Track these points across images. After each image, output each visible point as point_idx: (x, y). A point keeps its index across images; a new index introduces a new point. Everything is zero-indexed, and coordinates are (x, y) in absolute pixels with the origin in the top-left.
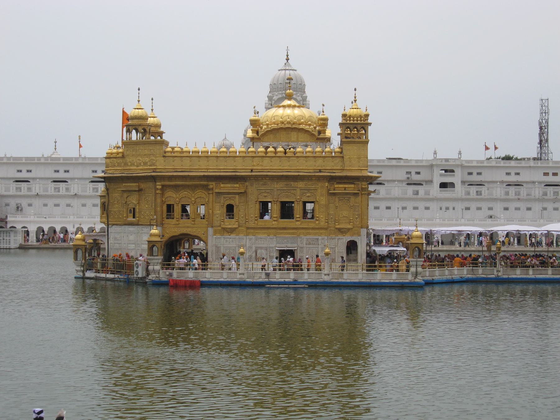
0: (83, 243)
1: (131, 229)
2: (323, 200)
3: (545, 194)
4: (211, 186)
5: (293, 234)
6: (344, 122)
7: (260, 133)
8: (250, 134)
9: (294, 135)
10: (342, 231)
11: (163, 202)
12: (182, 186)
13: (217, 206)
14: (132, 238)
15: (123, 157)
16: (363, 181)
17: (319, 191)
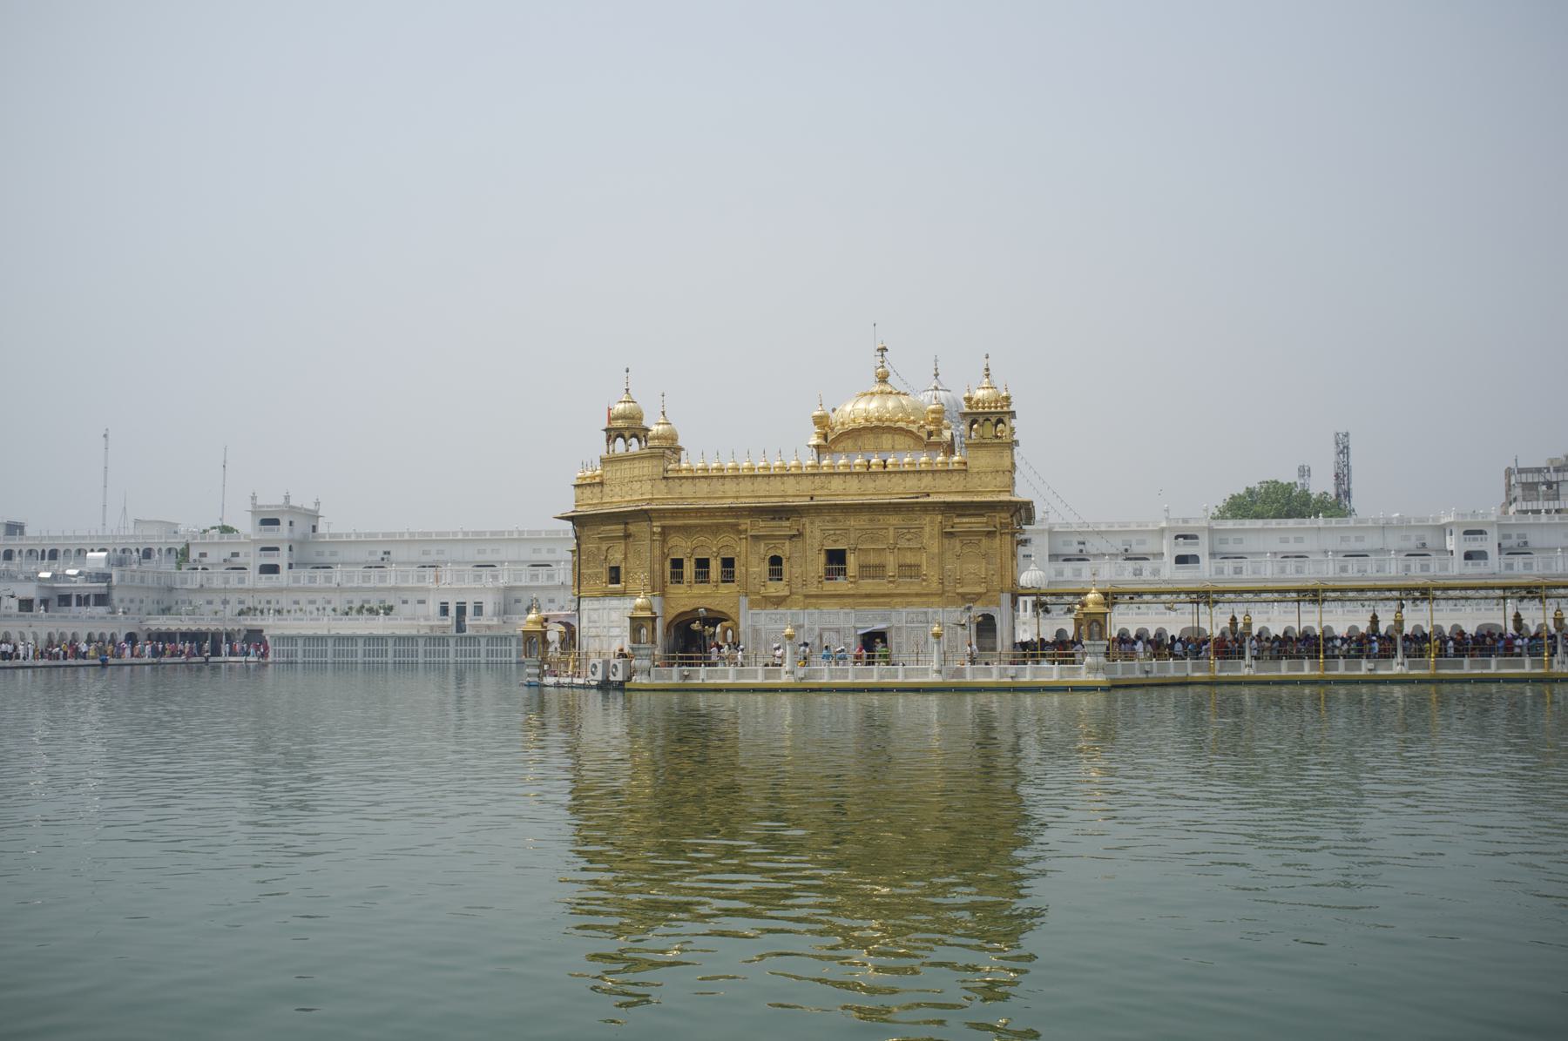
0: (539, 628)
1: (615, 603)
2: (934, 547)
3: (1344, 569)
4: (742, 527)
5: (884, 604)
6: (967, 410)
7: (831, 438)
8: (814, 441)
9: (886, 441)
10: (968, 599)
11: (664, 556)
12: (696, 526)
13: (754, 559)
14: (615, 616)
15: (601, 484)
16: (1002, 510)
17: (927, 529)
